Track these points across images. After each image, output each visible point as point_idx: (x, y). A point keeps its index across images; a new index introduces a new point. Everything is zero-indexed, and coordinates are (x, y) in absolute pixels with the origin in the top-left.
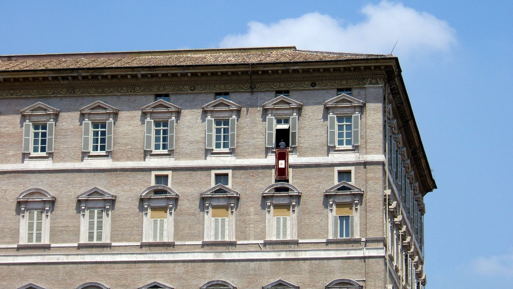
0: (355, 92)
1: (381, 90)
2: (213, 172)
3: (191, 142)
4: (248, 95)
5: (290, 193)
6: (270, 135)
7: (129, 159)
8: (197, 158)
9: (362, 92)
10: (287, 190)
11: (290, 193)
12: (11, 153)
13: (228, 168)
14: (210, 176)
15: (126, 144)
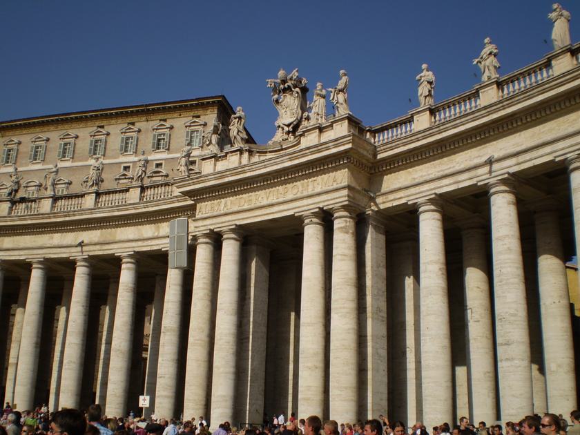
0: (202, 117)
1: (216, 115)
2: (123, 165)
3: (113, 150)
4: (145, 123)
5: (161, 174)
6: (154, 143)
7: (80, 161)
8: (115, 158)
9: (207, 117)
10: (159, 172)
11: (161, 174)
12: (24, 162)
13: (131, 162)
14: (120, 167)
15: (79, 154)
